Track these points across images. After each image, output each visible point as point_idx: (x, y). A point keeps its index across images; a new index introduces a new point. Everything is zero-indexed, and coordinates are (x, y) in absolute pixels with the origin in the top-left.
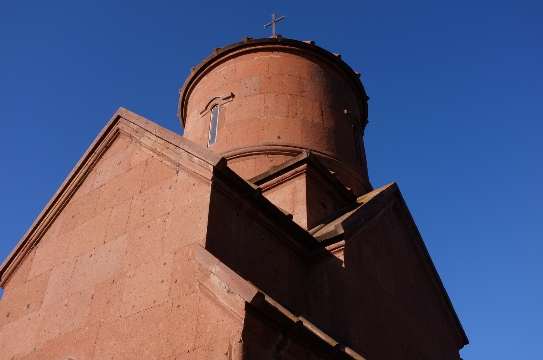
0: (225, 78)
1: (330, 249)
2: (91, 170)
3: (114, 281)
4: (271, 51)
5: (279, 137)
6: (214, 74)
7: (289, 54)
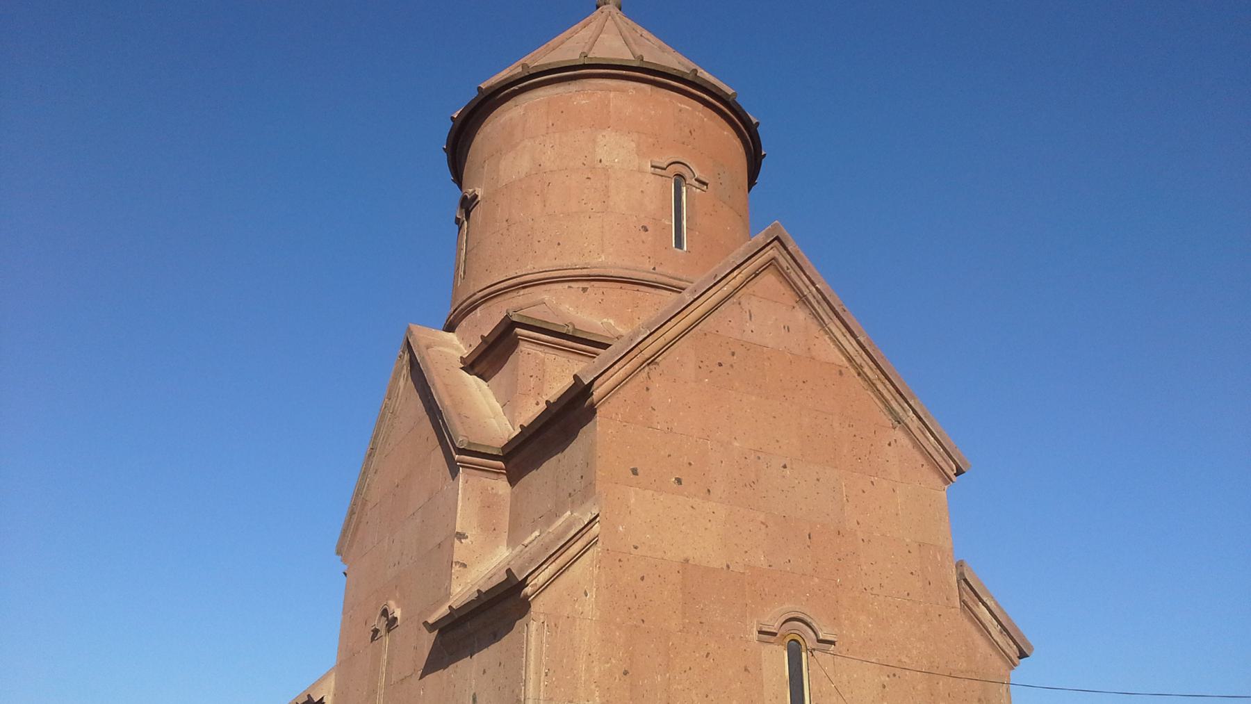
0: (690, 132)
3: (839, 532)
6: (667, 100)
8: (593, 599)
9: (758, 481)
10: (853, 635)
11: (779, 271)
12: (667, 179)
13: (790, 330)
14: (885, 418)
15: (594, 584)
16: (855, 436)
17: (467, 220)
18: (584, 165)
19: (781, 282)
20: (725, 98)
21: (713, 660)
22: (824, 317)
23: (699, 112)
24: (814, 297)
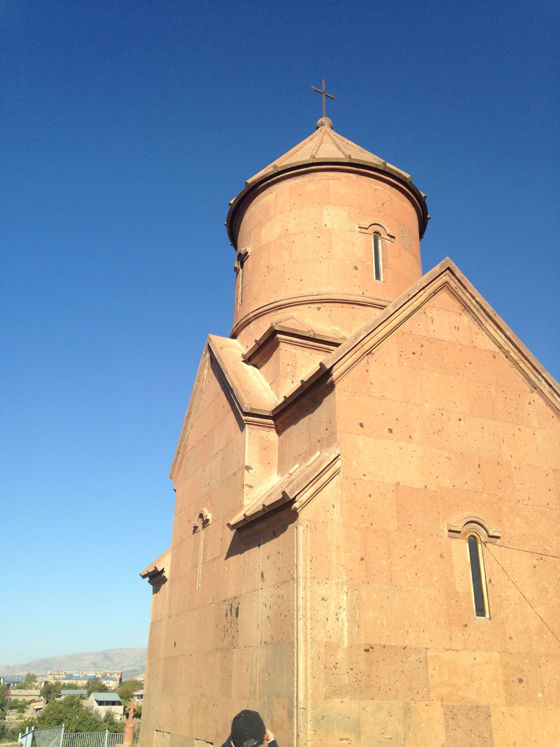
0: (383, 204)
3: (499, 463)
6: (367, 183)
8: (339, 510)
10: (512, 532)
11: (450, 290)
12: (368, 235)
13: (459, 329)
14: (525, 385)
15: (339, 500)
16: (506, 398)
17: (242, 268)
18: (315, 228)
19: (451, 297)
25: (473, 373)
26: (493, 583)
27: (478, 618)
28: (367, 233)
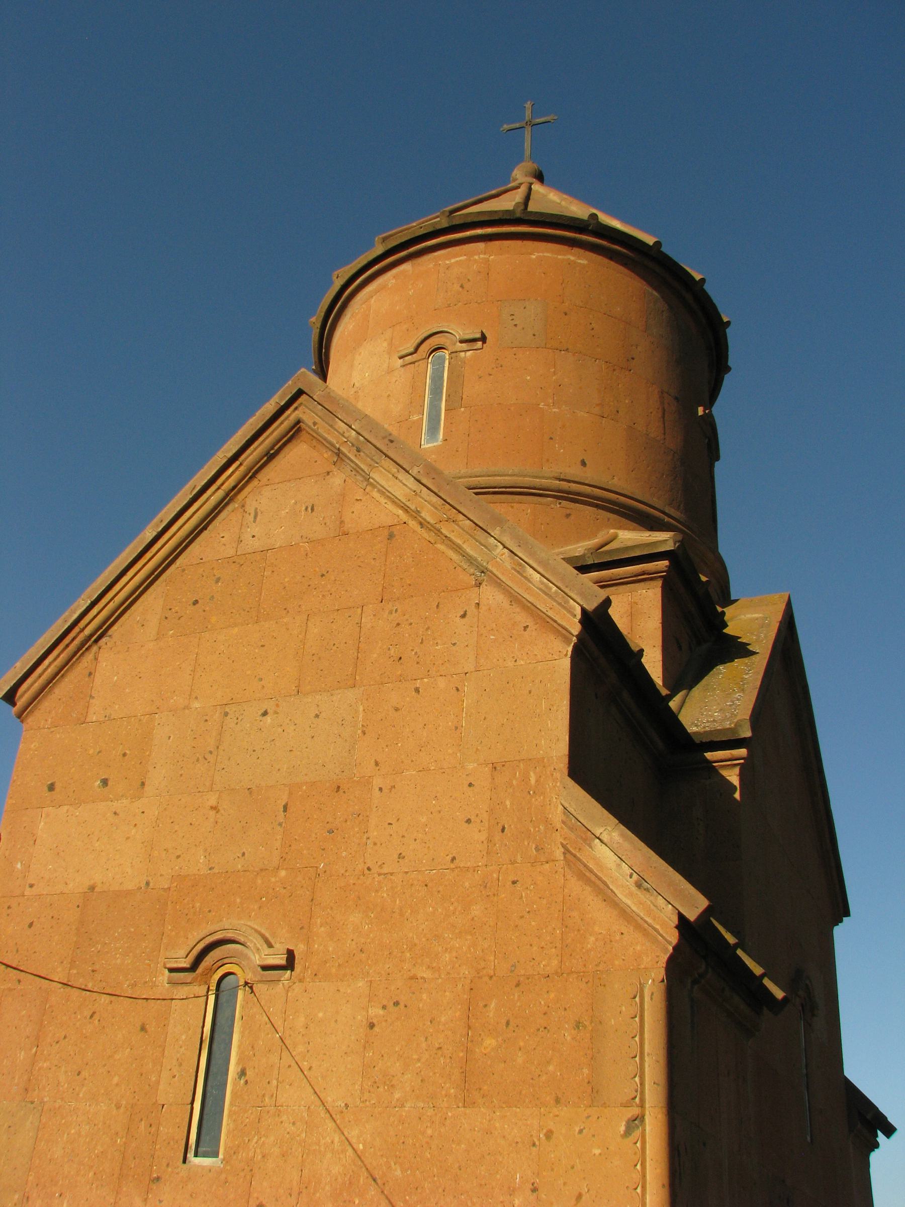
0: (462, 286)
1: (715, 759)
2: (231, 500)
3: (339, 787)
4: (569, 246)
5: (583, 463)
6: (431, 266)
7: (606, 261)
9: (218, 747)
10: (331, 949)
16: (398, 624)
20: (505, 217)
21: (99, 1021)
22: (362, 466)
23: (481, 253)
24: (352, 444)
25: (323, 596)
26: (247, 1078)
27: (198, 1160)
28: (416, 361)
